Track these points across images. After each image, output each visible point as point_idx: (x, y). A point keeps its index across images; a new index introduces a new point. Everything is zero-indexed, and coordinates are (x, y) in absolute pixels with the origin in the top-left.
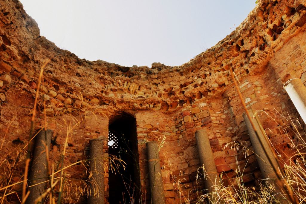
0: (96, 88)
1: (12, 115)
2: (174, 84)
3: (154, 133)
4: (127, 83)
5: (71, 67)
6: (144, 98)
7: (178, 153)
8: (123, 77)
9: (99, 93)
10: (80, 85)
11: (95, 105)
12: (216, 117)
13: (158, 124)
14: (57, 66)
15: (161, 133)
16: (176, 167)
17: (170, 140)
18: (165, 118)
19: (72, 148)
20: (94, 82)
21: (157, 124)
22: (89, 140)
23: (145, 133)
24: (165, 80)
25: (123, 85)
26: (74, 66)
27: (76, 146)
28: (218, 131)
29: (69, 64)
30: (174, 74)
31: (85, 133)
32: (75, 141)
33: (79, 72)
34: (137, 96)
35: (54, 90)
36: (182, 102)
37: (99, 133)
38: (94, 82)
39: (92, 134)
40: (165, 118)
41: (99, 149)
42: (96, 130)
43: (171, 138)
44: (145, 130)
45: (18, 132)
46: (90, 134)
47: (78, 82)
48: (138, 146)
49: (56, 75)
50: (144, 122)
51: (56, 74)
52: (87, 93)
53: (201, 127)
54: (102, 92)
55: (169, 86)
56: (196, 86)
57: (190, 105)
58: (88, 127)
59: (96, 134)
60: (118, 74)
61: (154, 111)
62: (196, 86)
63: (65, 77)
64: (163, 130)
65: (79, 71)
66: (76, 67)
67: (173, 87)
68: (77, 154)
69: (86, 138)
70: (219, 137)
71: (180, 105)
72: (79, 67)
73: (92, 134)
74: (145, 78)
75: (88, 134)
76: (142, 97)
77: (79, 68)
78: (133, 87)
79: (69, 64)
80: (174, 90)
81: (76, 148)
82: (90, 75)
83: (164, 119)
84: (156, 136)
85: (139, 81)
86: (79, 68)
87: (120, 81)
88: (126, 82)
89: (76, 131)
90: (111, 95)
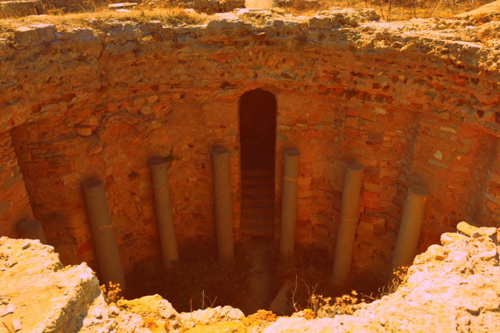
0: (214, 72)
2: (342, 68)
3: (300, 127)
4: (264, 54)
6: (291, 78)
8: (255, 46)
10: (187, 77)
12: (392, 137)
13: (308, 115)
14: (146, 68)
18: (321, 103)
20: (208, 64)
22: (213, 140)
23: (288, 125)
24: (326, 58)
25: (257, 58)
26: (171, 56)
28: (385, 159)
29: (163, 57)
30: (344, 53)
32: (195, 140)
33: (181, 58)
34: (279, 72)
36: (352, 93)
37: (225, 127)
38: (208, 64)
39: (216, 131)
40: (321, 103)
45: (129, 164)
46: (213, 130)
49: (150, 80)
53: (365, 144)
54: (223, 75)
55: (333, 68)
56: (376, 86)
58: (210, 123)
59: (220, 130)
60: (246, 44)
61: (306, 95)
62: (376, 86)
64: (314, 122)
65: (181, 57)
67: (340, 71)
69: (209, 139)
70: (384, 167)
72: (180, 50)
73: (216, 131)
74: (295, 47)
75: (211, 131)
76: (287, 75)
77: (179, 53)
78: (274, 59)
79: (163, 57)
80: (340, 76)
82: (200, 56)
85: (283, 53)
86: (179, 53)
87: (251, 53)
88: (261, 54)
90: (238, 75)
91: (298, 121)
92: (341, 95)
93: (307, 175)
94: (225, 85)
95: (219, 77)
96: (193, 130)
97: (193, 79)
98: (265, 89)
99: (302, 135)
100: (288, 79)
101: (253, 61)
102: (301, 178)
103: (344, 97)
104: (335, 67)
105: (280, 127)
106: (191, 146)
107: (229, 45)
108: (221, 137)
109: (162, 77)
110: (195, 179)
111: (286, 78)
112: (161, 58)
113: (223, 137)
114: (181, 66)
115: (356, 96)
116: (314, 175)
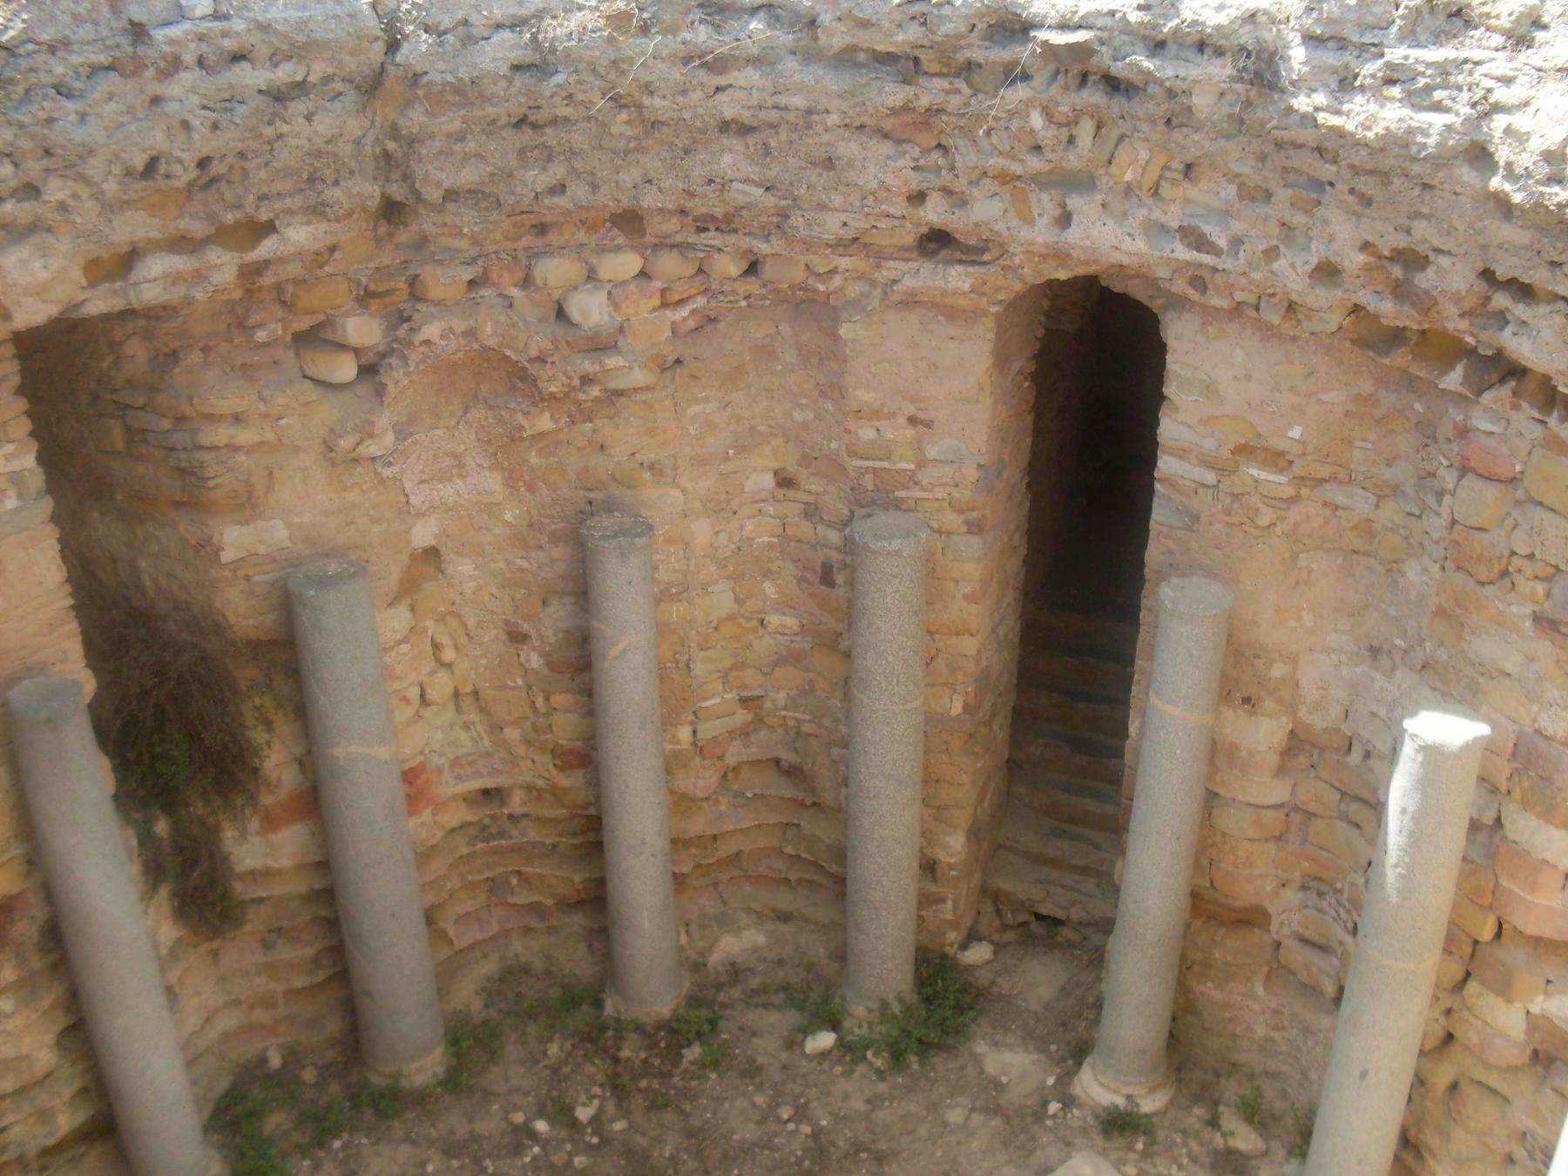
0: (874, 185)
1: (456, 456)
5: (670, 113)
7: (1374, 651)
8: (1054, 90)
9: (898, 214)
11: (891, 263)
13: (1296, 433)
14: (578, 139)
15: (1305, 492)
16: (1335, 712)
17: (1357, 543)
18: (1366, 387)
19: (791, 494)
20: (849, 148)
21: (1290, 434)
23: (1207, 462)
24: (1369, 186)
26: (680, 99)
27: (813, 488)
29: (646, 101)
31: (849, 432)
33: (729, 114)
34: (1173, 217)
35: (621, 240)
38: (849, 148)
40: (1366, 387)
41: (889, 599)
42: (911, 410)
43: (1367, 529)
44: (1209, 444)
45: (508, 517)
47: (749, 170)
48: (1147, 530)
50: (1210, 389)
51: (590, 179)
52: (816, 231)
53: (1528, 624)
57: (1537, 415)
58: (864, 396)
59: (910, 433)
61: (1294, 339)
63: (652, 175)
64: (1324, 472)
65: (729, 107)
66: (696, 96)
68: (819, 527)
69: (858, 463)
71: (1466, 381)
81: (811, 499)
83: (1360, 399)
84: (1263, 508)
85: (1177, 136)
87: (1037, 120)
89: (803, 401)
91: (1243, 450)
92: (1448, 366)
93: (1269, 705)
94: (937, 242)
95: (899, 207)
96: (798, 416)
97: (783, 203)
98: (1118, 288)
99: (1264, 521)
100: (1206, 259)
101: (1048, 155)
102: (1240, 712)
103: (1453, 380)
104: (1408, 231)
105: (1166, 464)
106: (785, 481)
107: (940, 75)
108: (912, 467)
109: (649, 181)
110: (791, 622)
111: (1198, 250)
112: (640, 107)
113: (920, 465)
114: (737, 144)
115: (1513, 383)
116: (1303, 714)
